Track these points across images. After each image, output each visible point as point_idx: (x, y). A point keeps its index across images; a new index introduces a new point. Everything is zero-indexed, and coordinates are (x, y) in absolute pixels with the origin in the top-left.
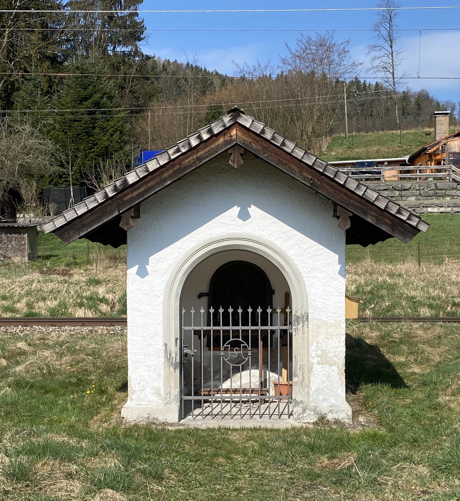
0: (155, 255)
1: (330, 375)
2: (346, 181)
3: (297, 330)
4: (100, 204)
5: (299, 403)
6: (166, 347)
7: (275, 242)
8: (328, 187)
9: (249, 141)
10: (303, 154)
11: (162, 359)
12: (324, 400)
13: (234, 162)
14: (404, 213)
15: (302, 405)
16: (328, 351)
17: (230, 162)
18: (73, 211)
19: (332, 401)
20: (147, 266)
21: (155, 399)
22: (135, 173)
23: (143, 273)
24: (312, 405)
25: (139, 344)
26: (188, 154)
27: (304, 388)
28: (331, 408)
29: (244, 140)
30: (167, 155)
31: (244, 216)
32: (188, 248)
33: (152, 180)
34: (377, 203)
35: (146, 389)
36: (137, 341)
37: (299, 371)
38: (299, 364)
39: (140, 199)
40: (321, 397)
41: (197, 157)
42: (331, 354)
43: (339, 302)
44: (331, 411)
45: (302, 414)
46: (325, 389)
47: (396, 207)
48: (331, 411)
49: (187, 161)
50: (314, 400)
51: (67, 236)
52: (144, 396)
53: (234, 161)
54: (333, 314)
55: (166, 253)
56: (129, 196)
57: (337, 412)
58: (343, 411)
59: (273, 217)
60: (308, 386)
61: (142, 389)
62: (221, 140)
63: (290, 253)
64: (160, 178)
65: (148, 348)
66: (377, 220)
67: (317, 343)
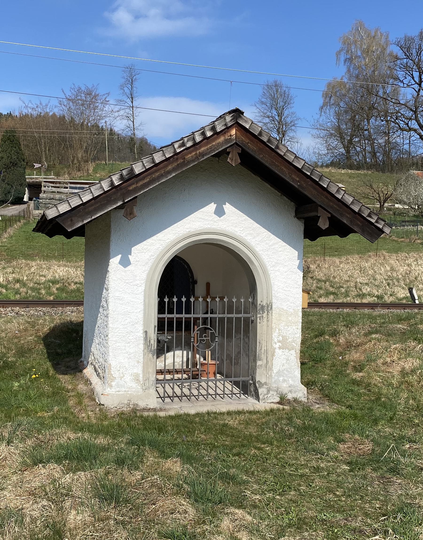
0: (138, 246)
1: (289, 358)
2: (328, 185)
3: (261, 318)
4: (105, 192)
5: (263, 385)
6: (146, 335)
7: (246, 238)
8: (312, 189)
9: (247, 142)
10: (293, 158)
11: (142, 346)
12: (284, 381)
13: (232, 160)
14: (373, 216)
15: (266, 387)
16: (287, 337)
17: (229, 160)
18: (78, 198)
19: (291, 382)
20: (129, 256)
21: (134, 385)
22: (141, 163)
23: (125, 263)
24: (274, 385)
25: (120, 332)
26: (191, 149)
27: (268, 371)
28: (290, 389)
29: (242, 141)
30: (173, 148)
31: (220, 212)
32: (168, 241)
33: (156, 171)
34: (352, 207)
35: (126, 375)
36: (118, 329)
37: (263, 355)
38: (263, 349)
39: (144, 189)
40: (281, 379)
41: (199, 153)
42: (290, 340)
43: (297, 294)
44: (290, 391)
45: (267, 394)
46: (285, 372)
47: (367, 211)
48: (290, 391)
49: (190, 155)
50: (275, 381)
51: (70, 222)
52: (124, 383)
53: (232, 159)
54: (292, 304)
55: (148, 244)
56: (134, 186)
57: (295, 392)
58: (301, 390)
59: (244, 215)
60: (271, 369)
61: (122, 376)
62: (222, 139)
63: (258, 249)
64: (164, 170)
65: (128, 335)
66: (351, 221)
67: (279, 330)
